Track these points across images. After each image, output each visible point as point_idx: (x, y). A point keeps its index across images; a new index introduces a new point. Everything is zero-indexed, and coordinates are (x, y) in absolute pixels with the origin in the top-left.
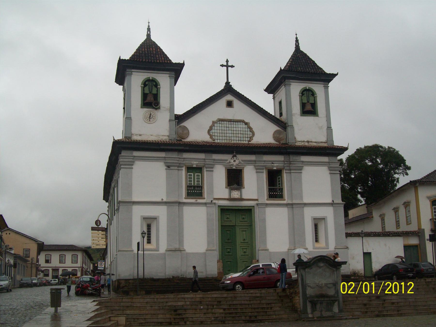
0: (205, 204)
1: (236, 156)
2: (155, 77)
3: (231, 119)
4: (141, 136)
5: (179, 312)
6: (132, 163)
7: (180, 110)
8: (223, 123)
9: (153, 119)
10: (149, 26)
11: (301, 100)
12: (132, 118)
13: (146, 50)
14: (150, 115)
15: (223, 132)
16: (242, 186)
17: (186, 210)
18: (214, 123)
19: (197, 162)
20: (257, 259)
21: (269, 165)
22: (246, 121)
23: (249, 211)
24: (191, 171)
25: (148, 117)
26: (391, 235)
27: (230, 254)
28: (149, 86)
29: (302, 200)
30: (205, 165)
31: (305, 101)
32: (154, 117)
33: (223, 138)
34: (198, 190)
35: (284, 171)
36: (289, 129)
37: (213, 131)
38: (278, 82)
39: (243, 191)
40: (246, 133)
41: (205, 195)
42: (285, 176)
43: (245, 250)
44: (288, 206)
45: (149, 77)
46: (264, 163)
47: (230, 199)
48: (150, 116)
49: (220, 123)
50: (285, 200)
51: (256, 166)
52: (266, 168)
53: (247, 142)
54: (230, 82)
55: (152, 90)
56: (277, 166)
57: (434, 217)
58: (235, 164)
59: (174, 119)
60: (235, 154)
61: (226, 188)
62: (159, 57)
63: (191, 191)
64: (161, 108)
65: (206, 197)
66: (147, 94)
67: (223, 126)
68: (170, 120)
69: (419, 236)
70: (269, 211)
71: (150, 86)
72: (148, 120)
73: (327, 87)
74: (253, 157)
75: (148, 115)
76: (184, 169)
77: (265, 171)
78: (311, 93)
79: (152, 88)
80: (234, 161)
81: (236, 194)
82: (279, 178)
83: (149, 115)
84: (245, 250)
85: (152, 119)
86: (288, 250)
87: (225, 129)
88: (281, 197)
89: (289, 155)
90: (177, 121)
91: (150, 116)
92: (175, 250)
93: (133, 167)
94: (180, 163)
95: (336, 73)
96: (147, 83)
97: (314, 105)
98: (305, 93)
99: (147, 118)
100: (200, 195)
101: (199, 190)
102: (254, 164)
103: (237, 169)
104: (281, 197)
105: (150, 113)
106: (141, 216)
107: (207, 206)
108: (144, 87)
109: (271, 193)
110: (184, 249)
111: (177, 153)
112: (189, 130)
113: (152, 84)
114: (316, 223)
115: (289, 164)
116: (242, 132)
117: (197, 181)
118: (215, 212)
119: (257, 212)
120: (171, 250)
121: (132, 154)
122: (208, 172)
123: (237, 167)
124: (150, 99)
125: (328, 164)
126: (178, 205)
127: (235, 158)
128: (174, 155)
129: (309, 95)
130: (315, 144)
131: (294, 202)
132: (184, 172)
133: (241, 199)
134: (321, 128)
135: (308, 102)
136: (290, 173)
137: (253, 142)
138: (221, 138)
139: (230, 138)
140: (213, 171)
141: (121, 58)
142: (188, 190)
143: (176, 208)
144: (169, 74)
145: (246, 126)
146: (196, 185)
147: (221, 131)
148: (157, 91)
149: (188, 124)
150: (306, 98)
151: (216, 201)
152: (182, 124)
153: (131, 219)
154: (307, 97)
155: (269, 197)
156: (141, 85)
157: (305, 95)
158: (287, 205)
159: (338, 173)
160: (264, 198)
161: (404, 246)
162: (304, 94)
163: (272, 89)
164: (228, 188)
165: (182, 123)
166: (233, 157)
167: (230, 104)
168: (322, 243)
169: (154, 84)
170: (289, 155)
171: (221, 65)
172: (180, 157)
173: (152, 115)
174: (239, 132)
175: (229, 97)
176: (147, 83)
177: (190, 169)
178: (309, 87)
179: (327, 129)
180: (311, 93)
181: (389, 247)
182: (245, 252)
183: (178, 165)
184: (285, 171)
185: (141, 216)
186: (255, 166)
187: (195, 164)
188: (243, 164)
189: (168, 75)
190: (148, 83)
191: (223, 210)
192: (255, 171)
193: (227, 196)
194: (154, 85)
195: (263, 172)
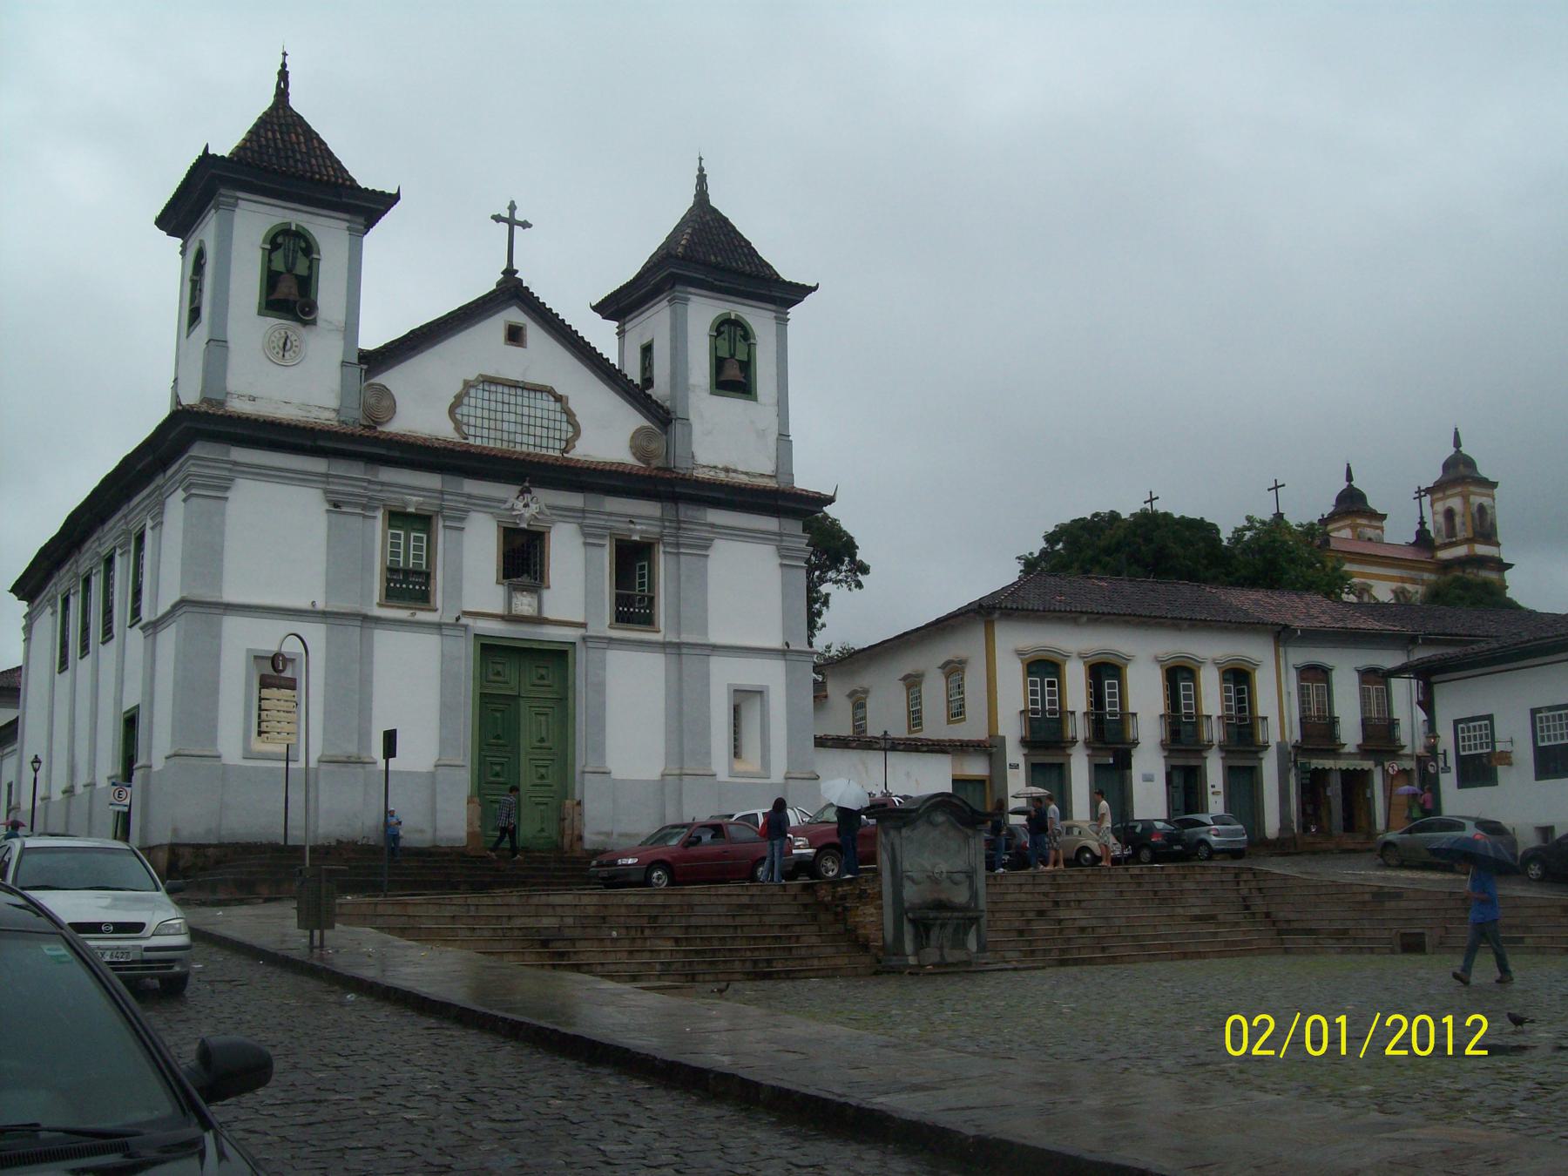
0: (439, 626)
1: (530, 492)
2: (306, 226)
3: (518, 381)
4: (254, 400)
5: (559, 946)
6: (224, 483)
7: (371, 338)
8: (493, 388)
9: (294, 352)
10: (284, 65)
11: (714, 349)
12: (231, 345)
13: (278, 136)
14: (286, 340)
15: (493, 415)
17: (384, 640)
18: (468, 385)
19: (421, 499)
20: (577, 798)
21: (621, 526)
22: (560, 391)
23: (558, 656)
24: (400, 524)
25: (278, 346)
26: (925, 749)
27: (501, 779)
28: (285, 249)
29: (706, 634)
30: (443, 508)
31: (724, 353)
32: (296, 346)
34: (417, 583)
36: (678, 428)
37: (465, 410)
38: (649, 287)
39: (546, 594)
40: (558, 425)
41: (439, 599)
42: (663, 564)
43: (543, 771)
44: (668, 650)
45: (286, 220)
46: (607, 521)
47: (511, 618)
48: (285, 344)
49: (486, 388)
50: (658, 632)
51: (587, 526)
52: (611, 535)
53: (557, 454)
54: (517, 271)
55: (294, 264)
56: (642, 532)
57: (1030, 707)
58: (527, 515)
59: (356, 361)
60: (527, 484)
61: (498, 583)
62: (319, 166)
63: (417, 587)
64: (319, 322)
65: (439, 604)
66: (281, 273)
68: (344, 364)
69: (990, 755)
70: (617, 660)
71: (289, 249)
72: (278, 353)
73: (782, 321)
74: (575, 500)
75: (278, 340)
76: (380, 514)
77: (607, 542)
78: (742, 333)
79: (294, 258)
80: (526, 505)
81: (524, 604)
82: (642, 568)
83: (283, 340)
84: (543, 771)
85: (291, 352)
86: (663, 775)
87: (500, 407)
88: (648, 621)
89: (676, 504)
90: (365, 367)
91: (285, 344)
92: (348, 762)
93: (228, 494)
94: (370, 498)
95: (814, 285)
96: (280, 240)
97: (747, 366)
98: (725, 328)
99: (274, 348)
101: (421, 584)
102: (580, 521)
103: (531, 528)
104: (648, 621)
105: (286, 333)
106: (248, 650)
107: (445, 632)
108: (271, 252)
109: (621, 609)
110: (372, 758)
111: (361, 465)
112: (397, 400)
113: (294, 244)
115: (676, 528)
116: (545, 423)
118: (465, 653)
119: (582, 660)
120: (335, 759)
121: (228, 453)
123: (532, 523)
124: (287, 289)
125: (778, 538)
127: (528, 497)
128: (356, 470)
129: (735, 335)
130: (744, 479)
131: (685, 638)
133: (539, 620)
134: (761, 434)
135: (732, 356)
138: (485, 433)
139: (512, 437)
140: (462, 529)
141: (211, 152)
142: (388, 581)
143: (354, 632)
144: (347, 221)
145: (558, 405)
146: (411, 566)
147: (486, 414)
148: (310, 268)
149: (393, 379)
150: (727, 343)
152: (377, 380)
153: (216, 657)
154: (730, 341)
155: (617, 620)
156: (264, 242)
157: (726, 336)
158: (664, 646)
159: (802, 567)
160: (602, 623)
161: (953, 780)
162: (723, 332)
163: (621, 305)
164: (503, 584)
165: (378, 374)
166: (522, 493)
168: (751, 761)
169: (303, 245)
170: (676, 504)
171: (494, 217)
172: (373, 479)
173: (291, 342)
174: (539, 422)
175: (515, 315)
176: (280, 240)
177: (397, 518)
178: (736, 315)
179: (777, 439)
180: (740, 332)
181: (916, 781)
182: (542, 777)
183: (364, 501)
184: (661, 548)
185: (248, 650)
186: (582, 526)
187: (413, 503)
188: (547, 516)
189: (346, 225)
190: (284, 240)
191: (489, 650)
192: (580, 540)
193: (499, 608)
195: (603, 546)
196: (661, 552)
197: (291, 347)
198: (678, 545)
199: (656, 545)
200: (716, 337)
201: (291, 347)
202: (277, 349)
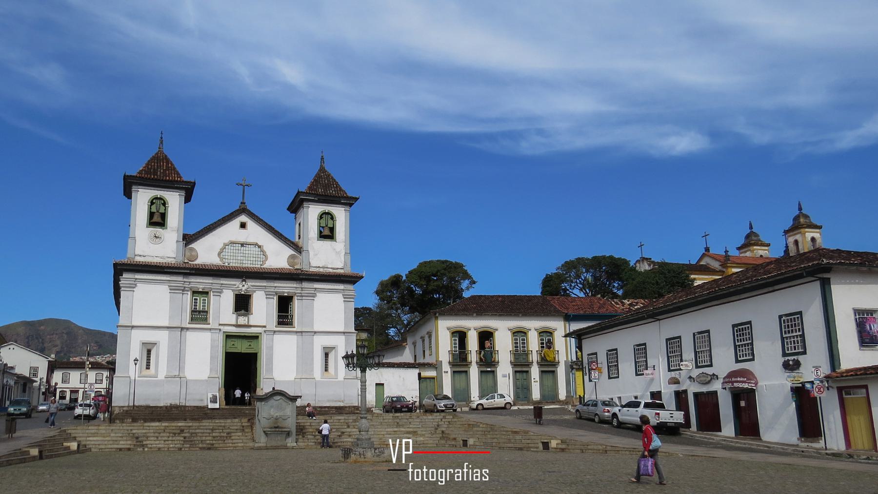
8: (234, 245)
33: (234, 261)
37: (224, 254)
53: (259, 266)
55: (159, 209)
66: (154, 213)
67: (235, 248)
98: (324, 216)
135: (327, 226)
137: (265, 266)
148: (165, 210)
156: (148, 202)
157: (324, 218)
169: (163, 202)
176: (154, 201)
194: (162, 204)
200: (320, 220)
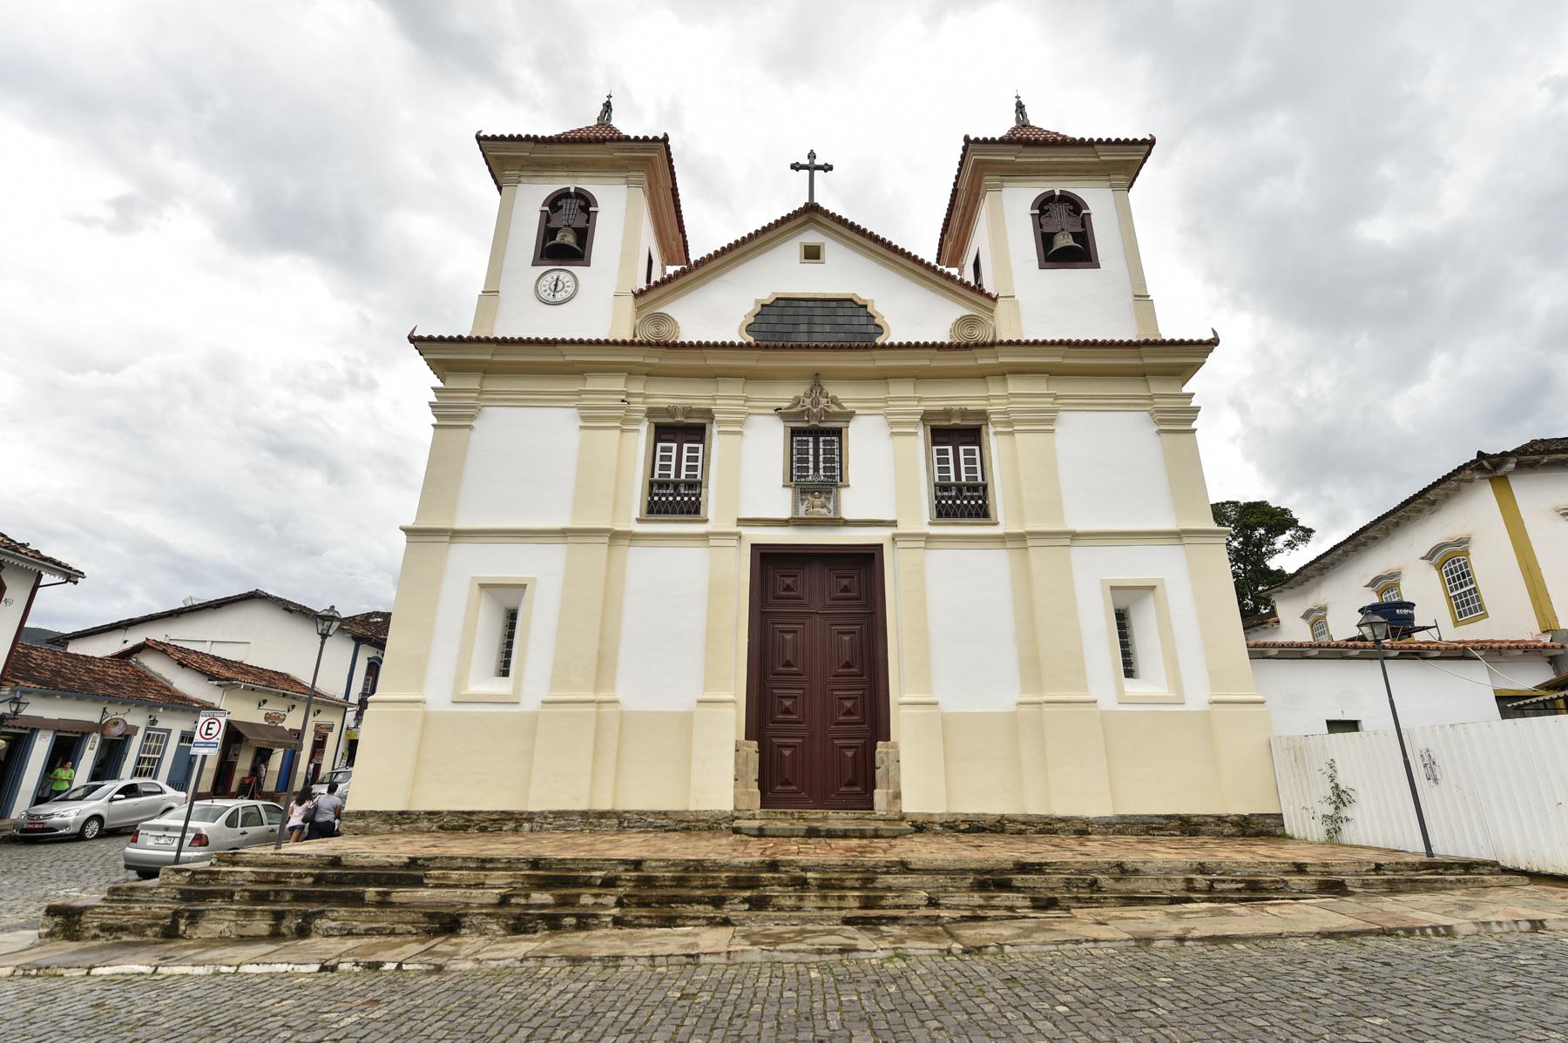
0: (705, 537)
16: (841, 480)
17: (638, 559)
23: (867, 561)
24: (671, 437)
25: (550, 288)
35: (987, 427)
44: (1009, 545)
48: (556, 285)
70: (939, 559)
77: (921, 432)
91: (556, 285)
100: (692, 509)
107: (712, 542)
114: (1122, 606)
117: (689, 468)
122: (722, 436)
126: (606, 540)
132: (641, 437)
136: (1012, 433)
143: (597, 551)
151: (745, 531)
155: (939, 515)
160: (919, 515)
164: (790, 486)
167: (812, 254)
189: (624, 180)
196: (991, 434)
197: (563, 288)
198: (1010, 423)
199: (984, 427)
201: (563, 288)
202: (549, 291)
